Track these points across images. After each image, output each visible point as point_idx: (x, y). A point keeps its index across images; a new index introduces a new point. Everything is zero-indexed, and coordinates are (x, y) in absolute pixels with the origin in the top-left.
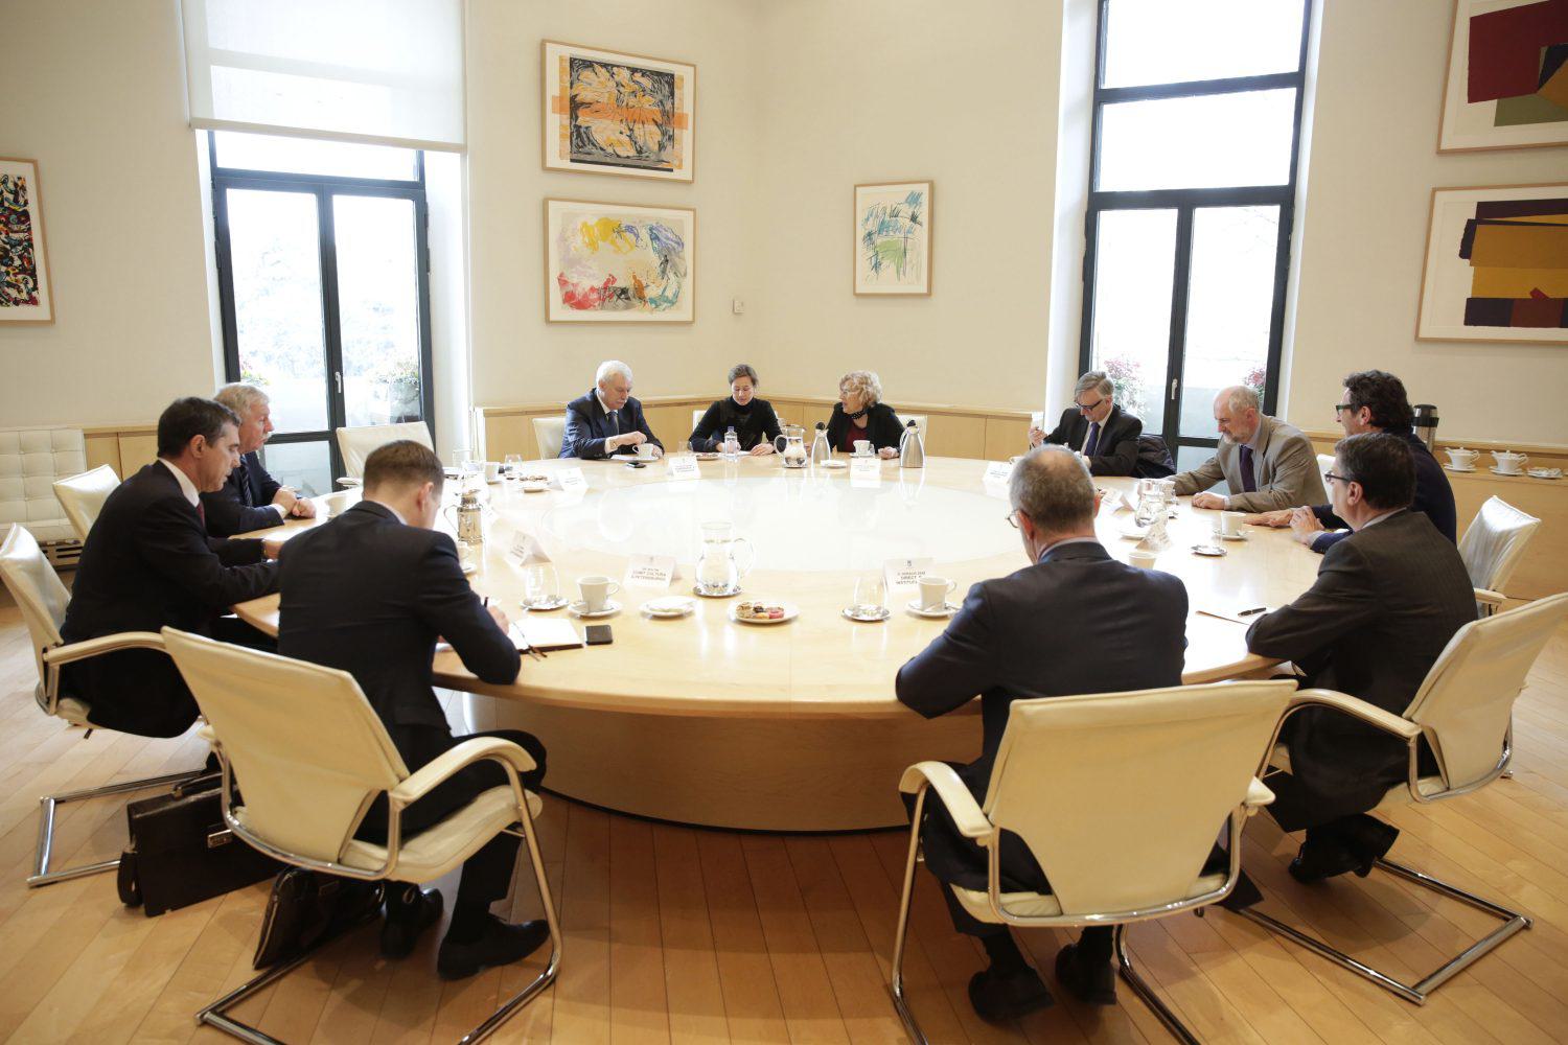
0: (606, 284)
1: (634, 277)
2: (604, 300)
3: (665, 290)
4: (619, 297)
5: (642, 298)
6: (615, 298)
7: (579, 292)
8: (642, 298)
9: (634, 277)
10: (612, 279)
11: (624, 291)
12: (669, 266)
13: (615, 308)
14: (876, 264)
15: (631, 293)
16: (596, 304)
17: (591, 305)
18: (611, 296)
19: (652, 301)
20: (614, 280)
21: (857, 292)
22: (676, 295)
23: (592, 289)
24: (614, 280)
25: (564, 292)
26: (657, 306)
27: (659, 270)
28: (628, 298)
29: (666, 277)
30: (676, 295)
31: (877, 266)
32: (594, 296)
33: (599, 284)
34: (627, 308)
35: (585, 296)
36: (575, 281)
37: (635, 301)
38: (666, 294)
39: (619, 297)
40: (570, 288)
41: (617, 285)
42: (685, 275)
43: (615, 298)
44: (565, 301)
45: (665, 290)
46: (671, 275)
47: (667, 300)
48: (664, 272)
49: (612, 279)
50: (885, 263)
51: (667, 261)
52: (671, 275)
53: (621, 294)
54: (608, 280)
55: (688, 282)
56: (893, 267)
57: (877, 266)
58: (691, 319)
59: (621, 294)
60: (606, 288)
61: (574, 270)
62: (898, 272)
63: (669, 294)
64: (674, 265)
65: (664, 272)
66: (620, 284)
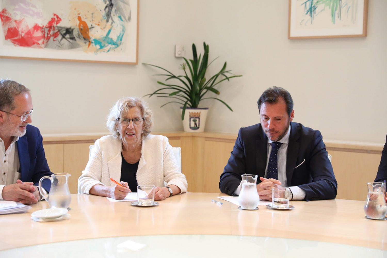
0: (51, 23)
1: (79, 18)
2: (48, 38)
3: (110, 31)
4: (64, 36)
5: (86, 38)
6: (60, 37)
7: (23, 29)
8: (86, 38)
9: (79, 18)
10: (56, 19)
11: (69, 31)
12: (113, 10)
13: (60, 47)
14: (311, 9)
15: (75, 33)
16: (40, 42)
17: (34, 43)
18: (55, 35)
19: (97, 42)
20: (59, 20)
21: (292, 35)
22: (120, 38)
23: (36, 27)
24: (59, 20)
25: (6, 29)
26: (101, 47)
27: (104, 13)
28: (73, 38)
29: (110, 21)
30: (120, 38)
31: (311, 10)
32: (38, 34)
33: (43, 22)
34: (72, 47)
35: (29, 33)
36: (18, 18)
37: (80, 42)
38: (111, 36)
39: (64, 36)
40: (13, 25)
41: (61, 24)
42: (129, 19)
43: (60, 37)
44: (7, 37)
45: (110, 31)
46: (116, 19)
47: (111, 42)
48: (108, 15)
49: (56, 19)
50: (320, 7)
51: (112, 5)
52: (116, 19)
53: (65, 34)
54: (53, 20)
55: (132, 27)
56: (328, 11)
57: (311, 10)
58: (134, 61)
59: (65, 34)
60: (50, 27)
61: (17, 7)
62: (333, 15)
63: (114, 36)
64: (118, 10)
65: (108, 15)
66: (65, 23)
